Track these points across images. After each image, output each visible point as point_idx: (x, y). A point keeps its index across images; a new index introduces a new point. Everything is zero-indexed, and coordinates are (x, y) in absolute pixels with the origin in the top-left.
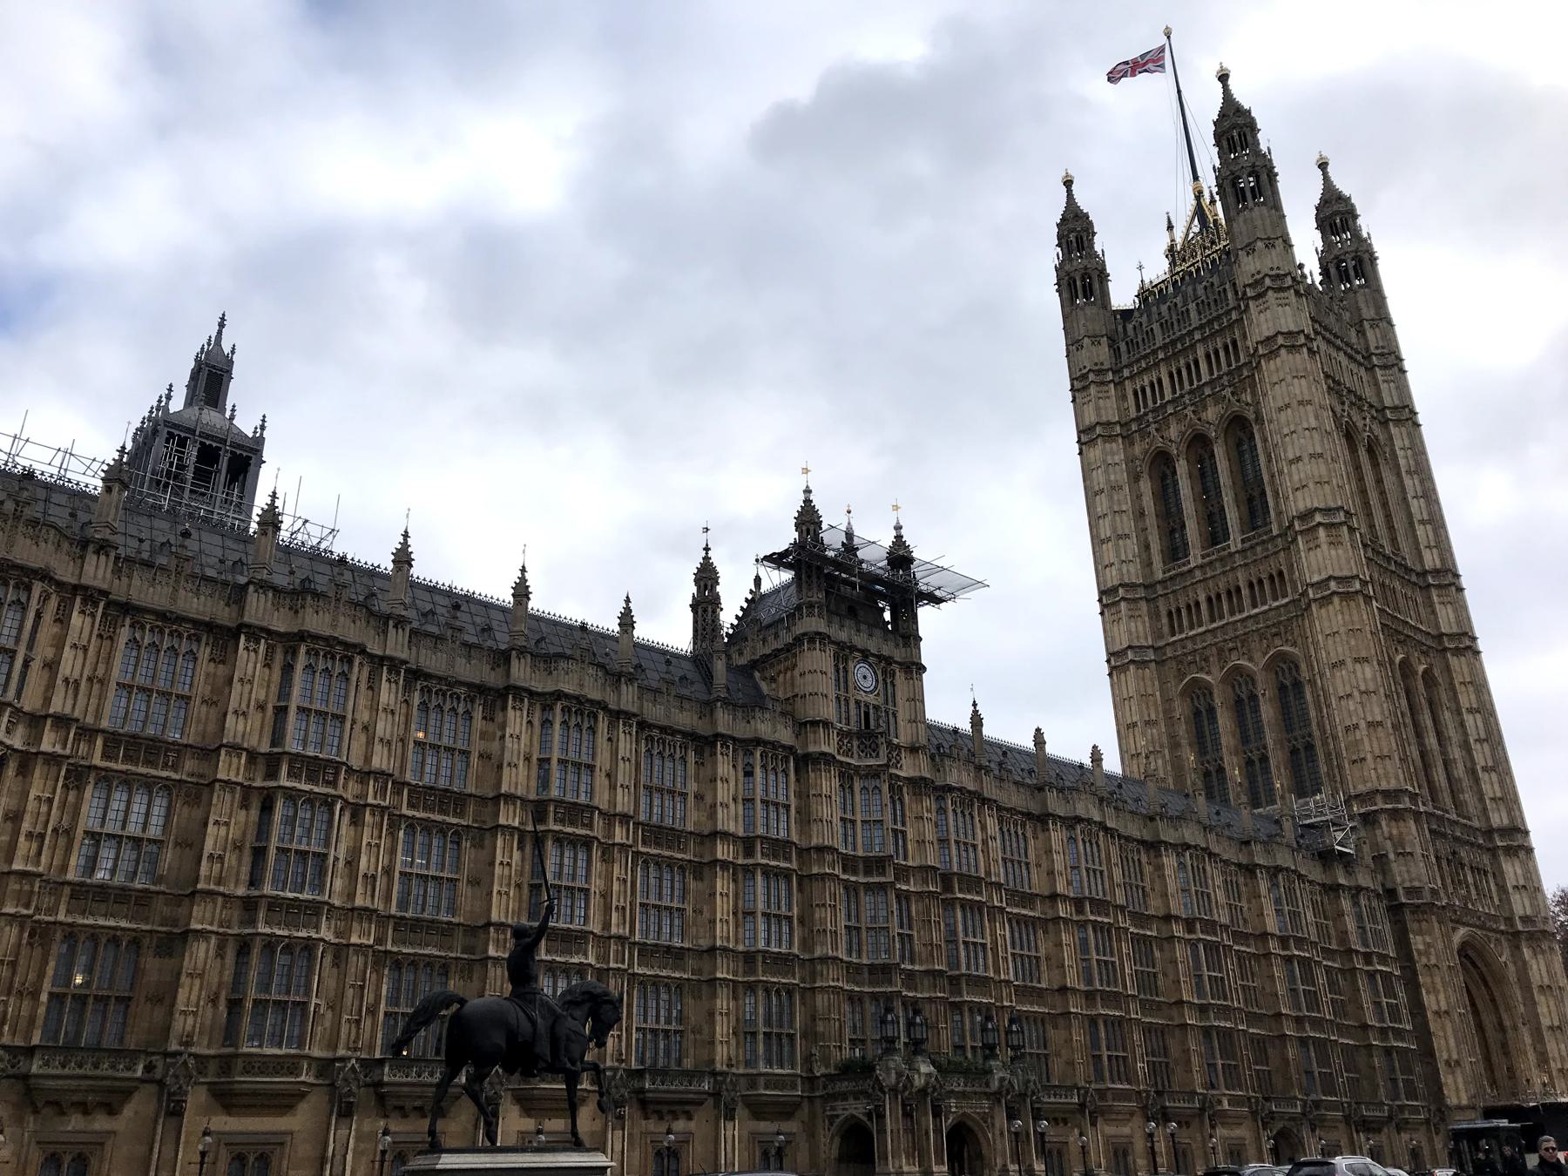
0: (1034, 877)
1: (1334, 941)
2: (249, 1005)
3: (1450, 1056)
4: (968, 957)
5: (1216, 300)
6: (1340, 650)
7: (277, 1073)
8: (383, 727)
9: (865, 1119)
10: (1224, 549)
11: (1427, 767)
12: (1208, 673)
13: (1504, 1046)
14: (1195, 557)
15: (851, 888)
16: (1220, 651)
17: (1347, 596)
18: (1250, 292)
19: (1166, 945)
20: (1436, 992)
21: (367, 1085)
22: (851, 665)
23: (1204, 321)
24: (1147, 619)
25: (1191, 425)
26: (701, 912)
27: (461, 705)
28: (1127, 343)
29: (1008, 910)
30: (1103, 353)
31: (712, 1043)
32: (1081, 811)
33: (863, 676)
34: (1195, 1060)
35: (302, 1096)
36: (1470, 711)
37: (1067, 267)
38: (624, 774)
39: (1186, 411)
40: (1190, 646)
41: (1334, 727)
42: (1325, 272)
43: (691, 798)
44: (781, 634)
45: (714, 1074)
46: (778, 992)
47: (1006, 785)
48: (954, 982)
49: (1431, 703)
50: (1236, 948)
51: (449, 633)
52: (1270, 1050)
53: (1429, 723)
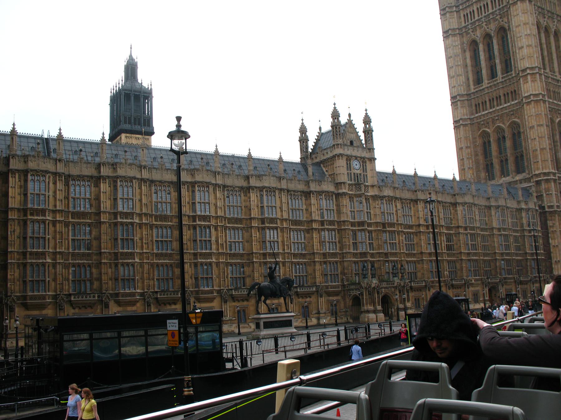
1: (519, 226)
3: (557, 258)
6: (533, 122)
7: (208, 294)
12: (489, 128)
14: (486, 83)
17: (537, 101)
19: (457, 235)
21: (230, 295)
22: (352, 161)
24: (467, 108)
25: (485, 30)
31: (315, 278)
33: (356, 165)
34: (464, 269)
35: (215, 298)
39: (483, 24)
40: (482, 117)
43: (304, 211)
45: (317, 286)
47: (404, 191)
48: (386, 255)
51: (232, 172)
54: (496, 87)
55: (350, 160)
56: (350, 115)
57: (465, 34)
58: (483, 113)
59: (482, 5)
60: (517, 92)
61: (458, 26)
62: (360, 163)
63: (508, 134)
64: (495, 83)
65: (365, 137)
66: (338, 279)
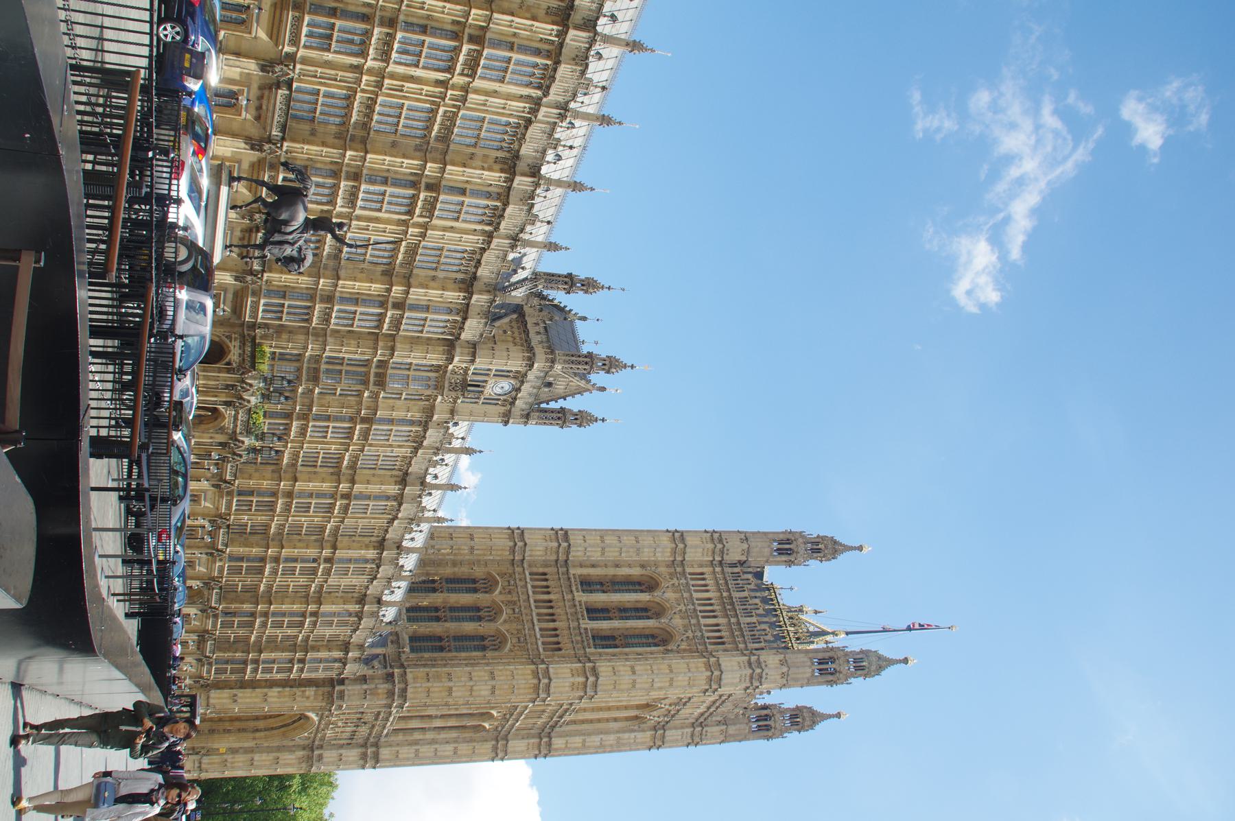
0: (367, 472)
2: (333, 21)
3: (241, 698)
4: (320, 427)
5: (754, 635)
6: (502, 678)
9: (227, 360)
10: (582, 616)
12: (501, 593)
13: (244, 730)
14: (582, 597)
15: (367, 363)
16: (515, 603)
17: (536, 688)
23: (742, 626)
24: (544, 558)
26: (362, 272)
27: (506, 145)
28: (739, 573)
29: (347, 454)
30: (734, 555)
33: (505, 385)
36: (456, 748)
37: (800, 540)
39: (682, 605)
40: (523, 583)
41: (453, 666)
42: (765, 707)
43: (433, 273)
44: (539, 336)
46: (308, 314)
48: (304, 417)
50: (313, 585)
52: (249, 594)
53: (449, 724)
54: (571, 614)
55: (515, 378)
56: (603, 389)
57: (673, 570)
59: (715, 607)
60: (556, 653)
61: (688, 561)
62: (505, 394)
64: (580, 616)
65: (553, 411)
66: (269, 319)
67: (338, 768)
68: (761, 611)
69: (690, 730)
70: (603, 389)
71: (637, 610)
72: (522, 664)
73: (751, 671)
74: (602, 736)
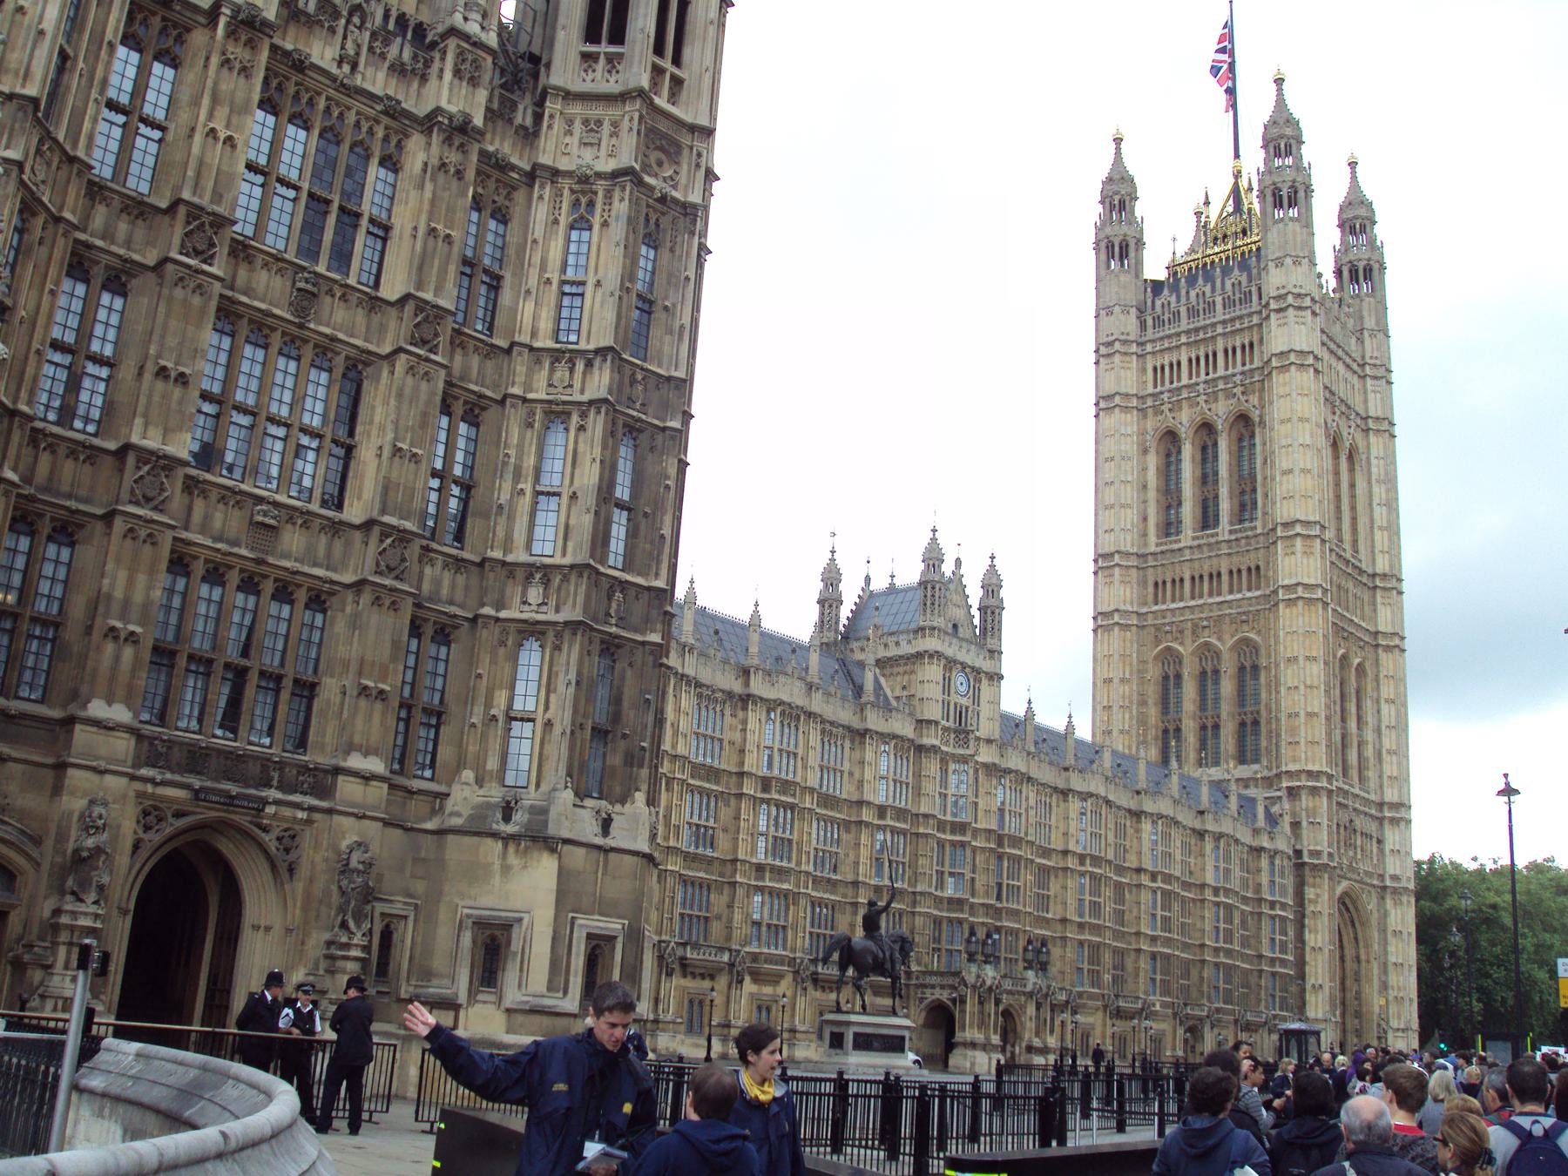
8: (683, 725)
11: (1344, 746)
12: (1181, 644)
14: (1188, 534)
16: (1195, 626)
17: (1310, 602)
18: (1273, 305)
20: (1316, 932)
30: (1130, 324)
32: (1092, 789)
33: (960, 681)
34: (1142, 974)
36: (1387, 701)
37: (1108, 231)
38: (814, 760)
41: (1278, 710)
42: (1338, 273)
43: (846, 776)
48: (997, 913)
49: (1358, 692)
53: (1354, 710)
56: (958, 562)
58: (1173, 606)
59: (1202, 355)
63: (1228, 666)
64: (1213, 540)
65: (983, 620)
67: (1409, 854)
68: (1208, 289)
69: (1369, 382)
70: (958, 562)
71: (1204, 460)
72: (1277, 618)
73: (1291, 310)
74: (1376, 501)
